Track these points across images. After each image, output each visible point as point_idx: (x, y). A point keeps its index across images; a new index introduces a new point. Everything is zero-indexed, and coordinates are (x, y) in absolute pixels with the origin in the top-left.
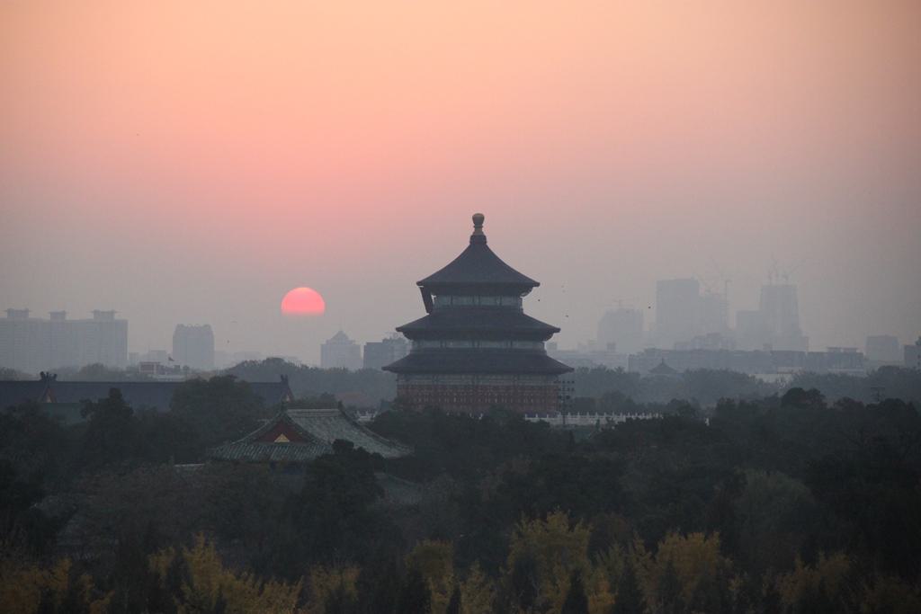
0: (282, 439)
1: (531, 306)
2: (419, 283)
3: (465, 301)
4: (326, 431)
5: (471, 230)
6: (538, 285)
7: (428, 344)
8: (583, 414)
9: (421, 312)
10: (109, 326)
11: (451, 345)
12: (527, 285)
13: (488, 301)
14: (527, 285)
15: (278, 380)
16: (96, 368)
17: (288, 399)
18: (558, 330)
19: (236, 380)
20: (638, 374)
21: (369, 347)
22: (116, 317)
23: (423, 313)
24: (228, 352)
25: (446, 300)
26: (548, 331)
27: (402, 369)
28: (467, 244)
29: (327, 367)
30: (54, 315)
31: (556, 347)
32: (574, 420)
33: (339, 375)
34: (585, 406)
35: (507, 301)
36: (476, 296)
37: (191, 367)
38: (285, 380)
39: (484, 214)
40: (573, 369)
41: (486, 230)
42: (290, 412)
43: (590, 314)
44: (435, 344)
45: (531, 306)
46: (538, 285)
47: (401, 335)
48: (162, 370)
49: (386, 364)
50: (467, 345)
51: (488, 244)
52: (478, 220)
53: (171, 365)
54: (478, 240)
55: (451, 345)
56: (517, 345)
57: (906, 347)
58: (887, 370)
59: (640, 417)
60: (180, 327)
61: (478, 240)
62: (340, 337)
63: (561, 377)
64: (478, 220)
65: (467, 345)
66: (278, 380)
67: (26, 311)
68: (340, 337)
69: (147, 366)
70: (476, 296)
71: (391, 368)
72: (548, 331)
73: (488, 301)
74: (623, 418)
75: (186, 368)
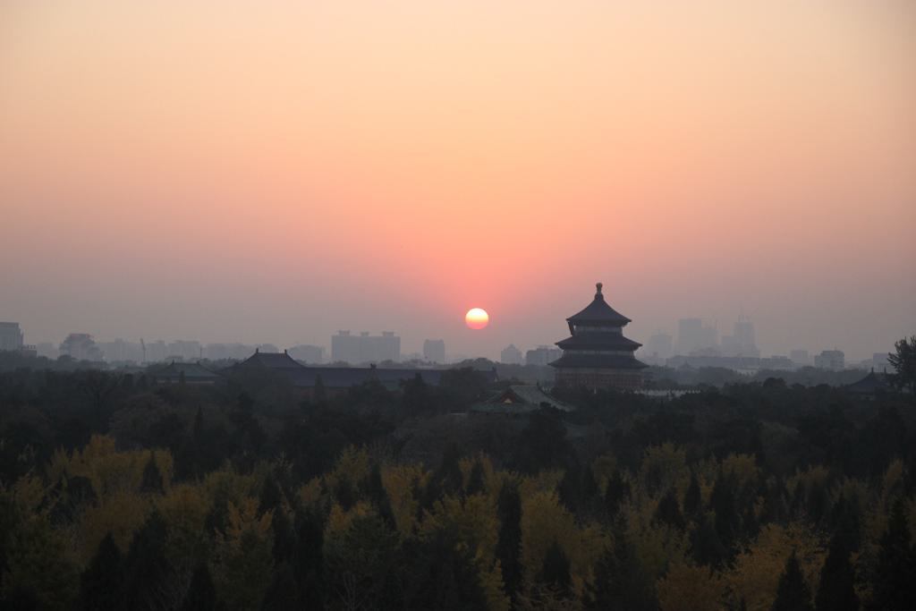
0: (508, 401)
1: (627, 332)
2: (567, 320)
3: (592, 329)
4: (534, 399)
5: (596, 292)
6: (630, 321)
7: (571, 352)
8: (653, 389)
9: (568, 335)
10: (391, 340)
11: (585, 352)
12: (625, 321)
13: (604, 329)
14: (625, 321)
15: (491, 369)
16: (389, 362)
17: (496, 380)
18: (641, 345)
19: (475, 369)
20: (674, 369)
21: (529, 353)
22: (395, 335)
23: (568, 335)
24: (454, 354)
25: (582, 329)
26: (636, 346)
27: (557, 365)
28: (592, 299)
29: (505, 362)
30: (363, 334)
31: (638, 354)
32: (651, 393)
33: (515, 367)
34: (650, 385)
35: (615, 330)
36: (598, 325)
37: (437, 362)
38: (494, 370)
39: (603, 283)
40: (648, 366)
41: (603, 292)
42: (513, 387)
43: (655, 337)
44: (575, 352)
45: (627, 332)
46: (630, 321)
47: (557, 346)
48: (422, 363)
49: (550, 361)
50: (592, 352)
51: (605, 299)
52: (599, 286)
53: (427, 361)
54: (599, 297)
55: (585, 352)
56: (620, 353)
57: (816, 357)
58: (808, 368)
59: (690, 392)
60: (427, 341)
61: (599, 297)
62: (512, 346)
63: (643, 370)
64: (599, 286)
65: (592, 352)
66: (491, 369)
67: (348, 332)
68: (512, 346)
69: (415, 361)
70: (598, 325)
71: (553, 364)
72: (636, 346)
73: (604, 329)
74: (683, 393)
75: (435, 363)
